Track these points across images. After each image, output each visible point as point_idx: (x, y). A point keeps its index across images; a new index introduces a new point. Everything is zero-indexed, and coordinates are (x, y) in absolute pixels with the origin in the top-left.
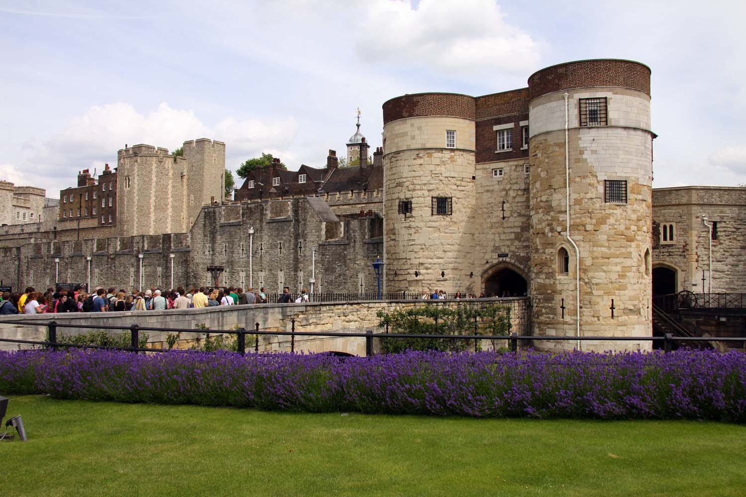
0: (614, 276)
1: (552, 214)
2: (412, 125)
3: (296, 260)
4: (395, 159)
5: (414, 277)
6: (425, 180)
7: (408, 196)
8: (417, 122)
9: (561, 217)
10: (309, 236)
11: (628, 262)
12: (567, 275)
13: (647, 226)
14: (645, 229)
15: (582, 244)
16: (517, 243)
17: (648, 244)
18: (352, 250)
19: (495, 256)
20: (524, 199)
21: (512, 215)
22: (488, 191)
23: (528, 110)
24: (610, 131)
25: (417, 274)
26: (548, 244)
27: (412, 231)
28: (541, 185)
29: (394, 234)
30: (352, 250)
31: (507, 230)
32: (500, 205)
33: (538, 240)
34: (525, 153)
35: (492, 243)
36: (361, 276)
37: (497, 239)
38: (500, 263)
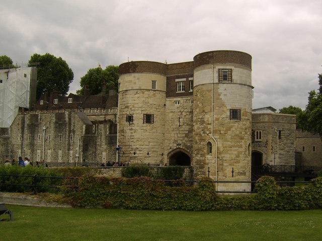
0: (233, 156)
3: (69, 145)
5: (133, 155)
6: (140, 105)
8: (137, 75)
9: (209, 126)
11: (241, 150)
13: (249, 132)
14: (248, 133)
15: (219, 140)
16: (186, 139)
17: (250, 141)
18: (99, 140)
19: (175, 145)
22: (172, 112)
23: (193, 72)
24: (232, 85)
25: (135, 153)
27: (133, 131)
28: (199, 110)
32: (178, 119)
33: (197, 138)
34: (191, 94)
35: (173, 139)
36: (104, 154)
37: (176, 136)
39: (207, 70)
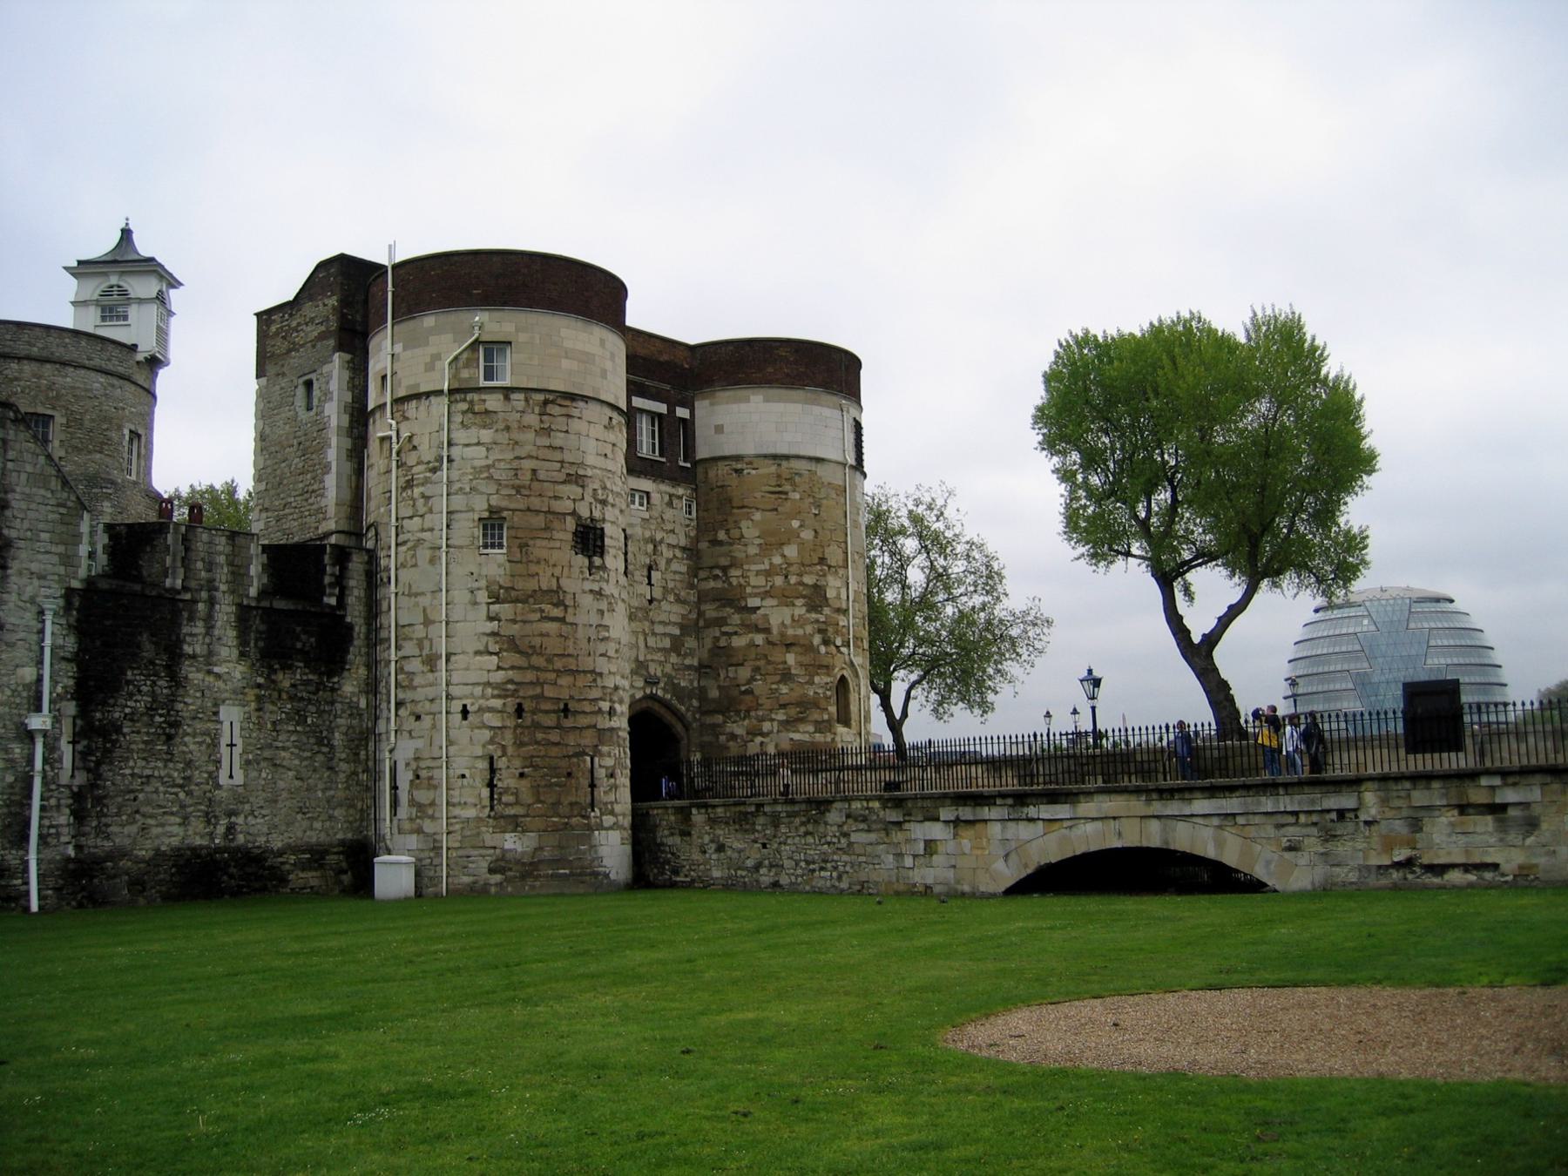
1: (827, 611)
2: (602, 342)
4: (564, 411)
7: (597, 514)
10: (23, 555)
16: (674, 659)
18: (199, 628)
19: (640, 683)
20: (684, 569)
21: (664, 598)
26: (821, 667)
27: (604, 605)
29: (556, 605)
30: (199, 628)
31: (659, 629)
32: (645, 573)
33: (791, 659)
36: (231, 715)
38: (646, 697)
39: (827, 412)
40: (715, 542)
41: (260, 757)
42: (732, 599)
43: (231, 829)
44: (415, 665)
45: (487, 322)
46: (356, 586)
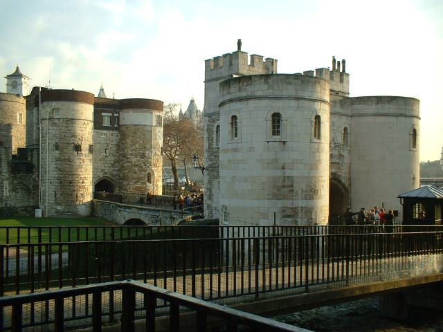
7: (80, 143)
12: (150, 183)
16: (112, 168)
25: (83, 183)
33: (136, 169)
40: (122, 143)
41: (14, 190)
42: (124, 156)
43: (6, 204)
44: (43, 173)
45: (54, 104)
46: (35, 156)
